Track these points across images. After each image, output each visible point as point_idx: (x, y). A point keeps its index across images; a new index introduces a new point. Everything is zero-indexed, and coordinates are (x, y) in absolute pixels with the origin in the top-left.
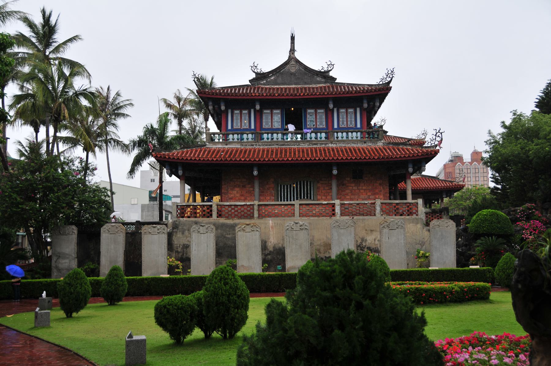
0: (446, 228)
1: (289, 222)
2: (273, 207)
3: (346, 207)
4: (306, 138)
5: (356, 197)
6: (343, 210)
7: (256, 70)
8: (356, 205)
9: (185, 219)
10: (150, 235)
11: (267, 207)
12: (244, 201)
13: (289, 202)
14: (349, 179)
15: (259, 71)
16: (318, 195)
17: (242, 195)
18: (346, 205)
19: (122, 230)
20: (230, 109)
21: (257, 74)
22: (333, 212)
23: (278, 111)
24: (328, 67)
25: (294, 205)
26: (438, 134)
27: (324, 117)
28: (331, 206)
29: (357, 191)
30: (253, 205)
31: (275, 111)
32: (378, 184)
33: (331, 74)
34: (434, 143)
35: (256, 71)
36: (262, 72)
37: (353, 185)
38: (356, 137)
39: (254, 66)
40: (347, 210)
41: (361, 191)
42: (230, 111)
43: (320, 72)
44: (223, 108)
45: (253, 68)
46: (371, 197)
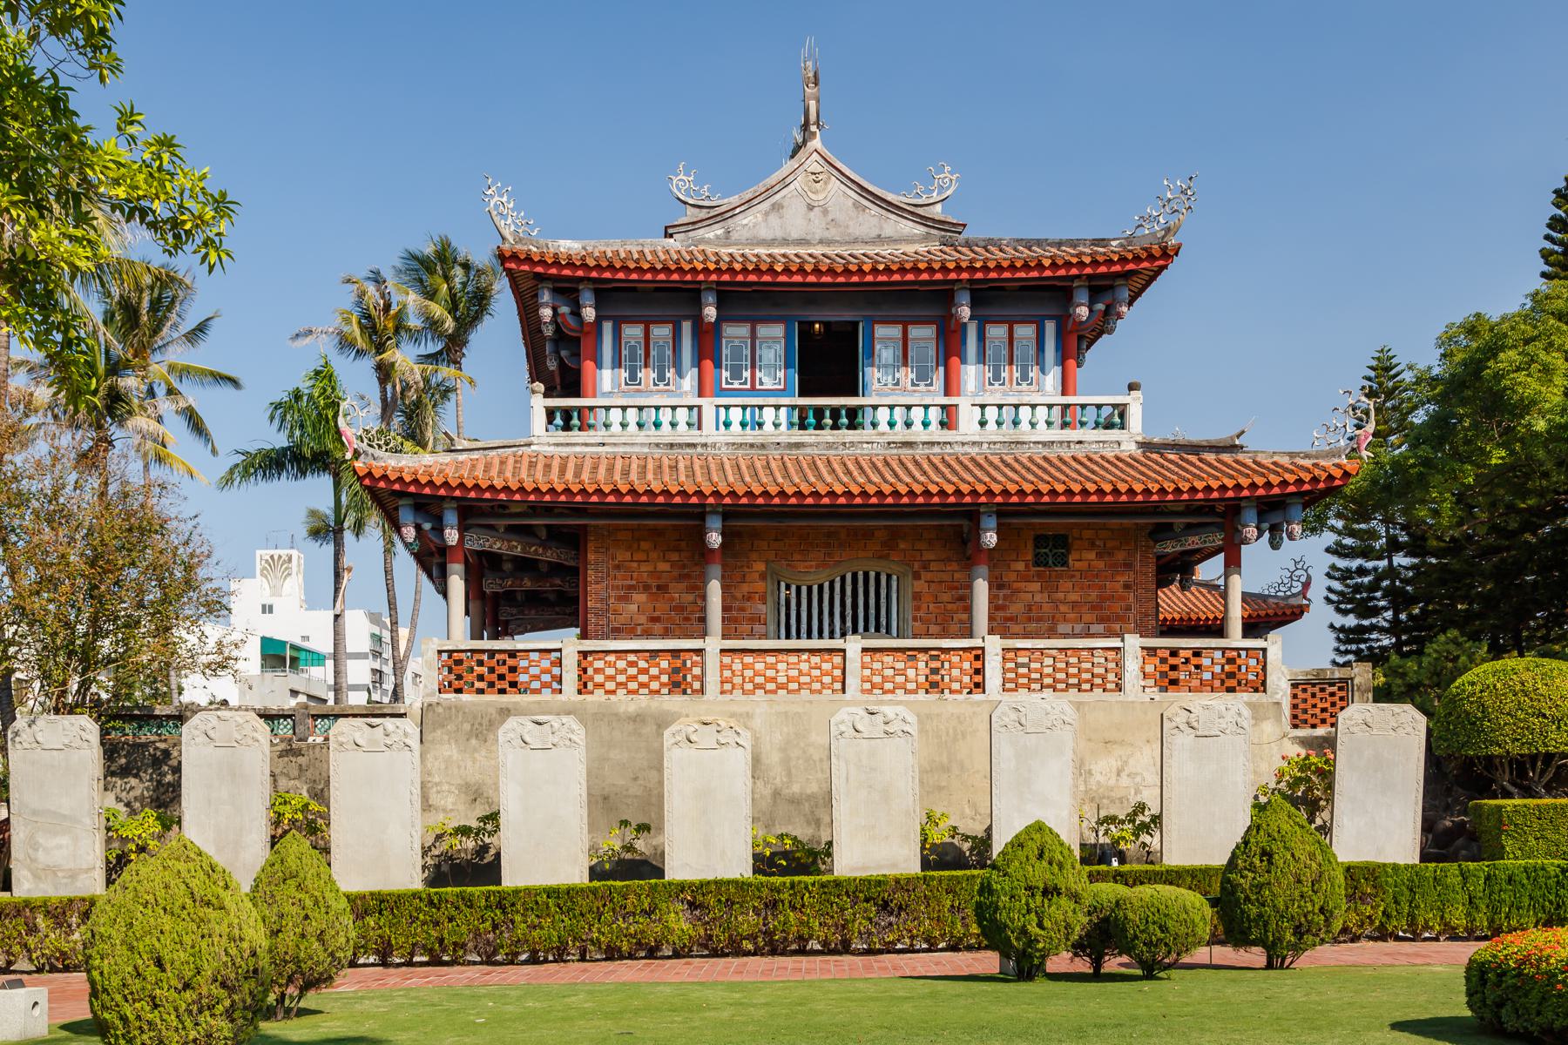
0: (1391, 732)
1: (849, 711)
2: (771, 659)
3: (1020, 660)
4: (874, 425)
5: (1045, 625)
6: (1010, 670)
8: (1054, 652)
9: (465, 697)
10: (360, 754)
11: (748, 659)
12: (666, 634)
13: (826, 643)
14: (1020, 566)
16: (915, 619)
17: (654, 620)
18: (1023, 652)
19: (255, 735)
20: (608, 318)
22: (978, 679)
23: (778, 330)
25: (844, 651)
28: (972, 657)
29: (1047, 608)
30: (699, 652)
31: (763, 331)
32: (1119, 586)
37: (1036, 586)
38: (1030, 423)
40: (1023, 670)
41: (1063, 608)
42: (607, 327)
44: (589, 314)
46: (1096, 628)
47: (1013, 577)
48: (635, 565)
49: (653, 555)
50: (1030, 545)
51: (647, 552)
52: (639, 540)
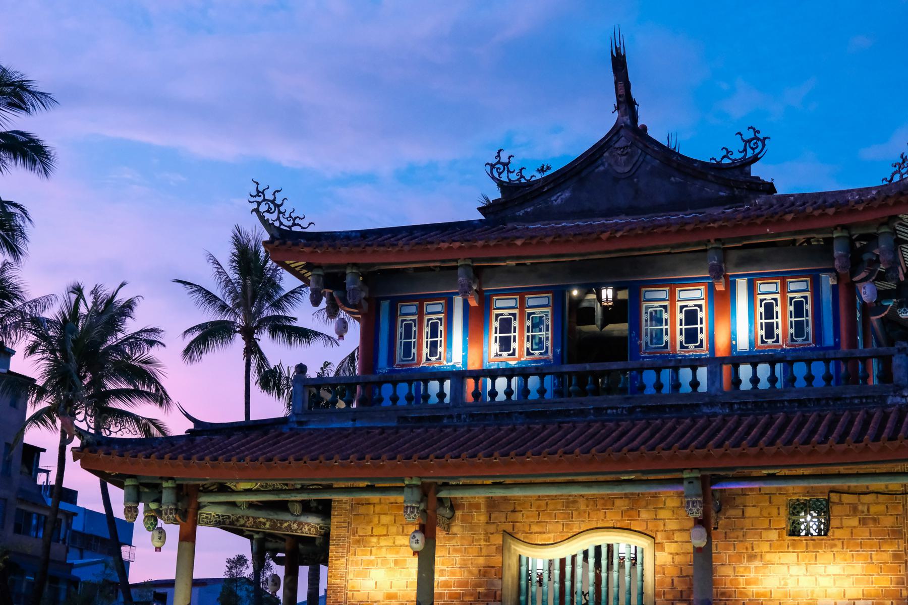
7: (505, 174)
14: (773, 535)
15: (514, 177)
24: (745, 150)
33: (756, 170)
35: (504, 178)
36: (523, 181)
37: (791, 557)
39: (499, 163)
43: (717, 167)
45: (494, 171)
47: (765, 547)
48: (374, 540)
49: (393, 529)
50: (784, 512)
51: (387, 526)
52: (379, 514)
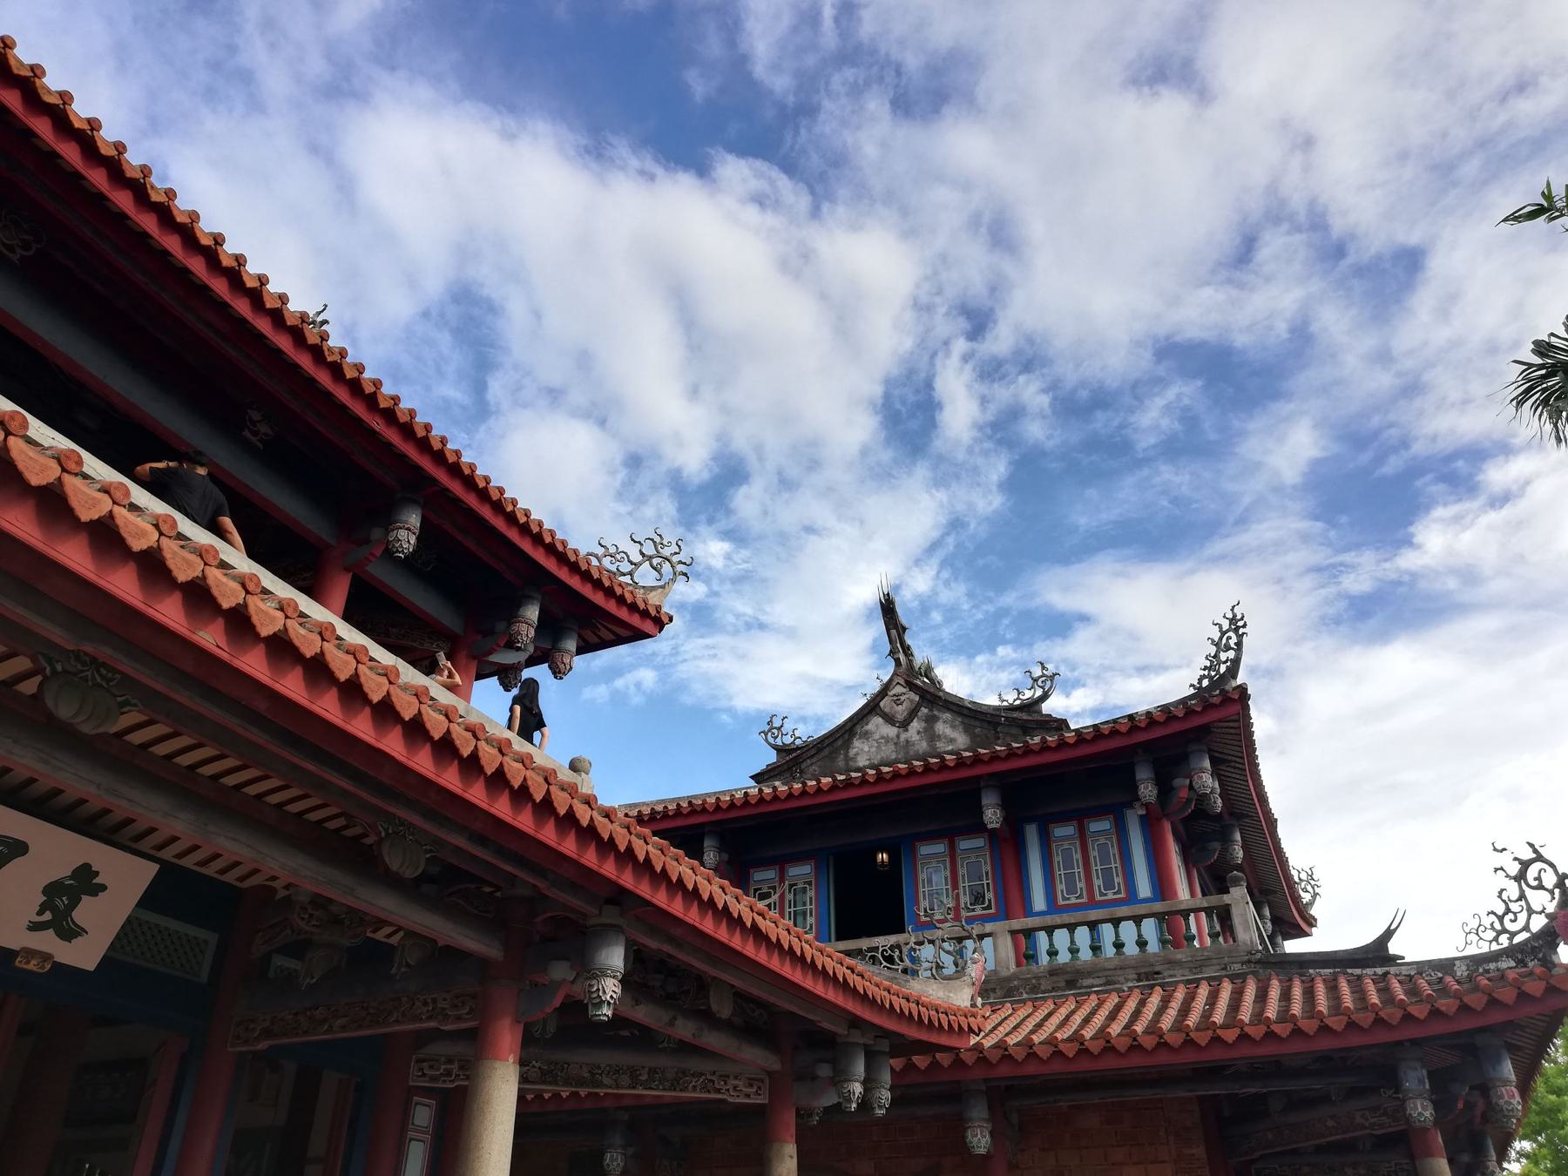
7: (778, 739)
15: (788, 740)
21: (780, 750)
26: (1532, 872)
27: (987, 867)
34: (1526, 928)
36: (798, 742)
